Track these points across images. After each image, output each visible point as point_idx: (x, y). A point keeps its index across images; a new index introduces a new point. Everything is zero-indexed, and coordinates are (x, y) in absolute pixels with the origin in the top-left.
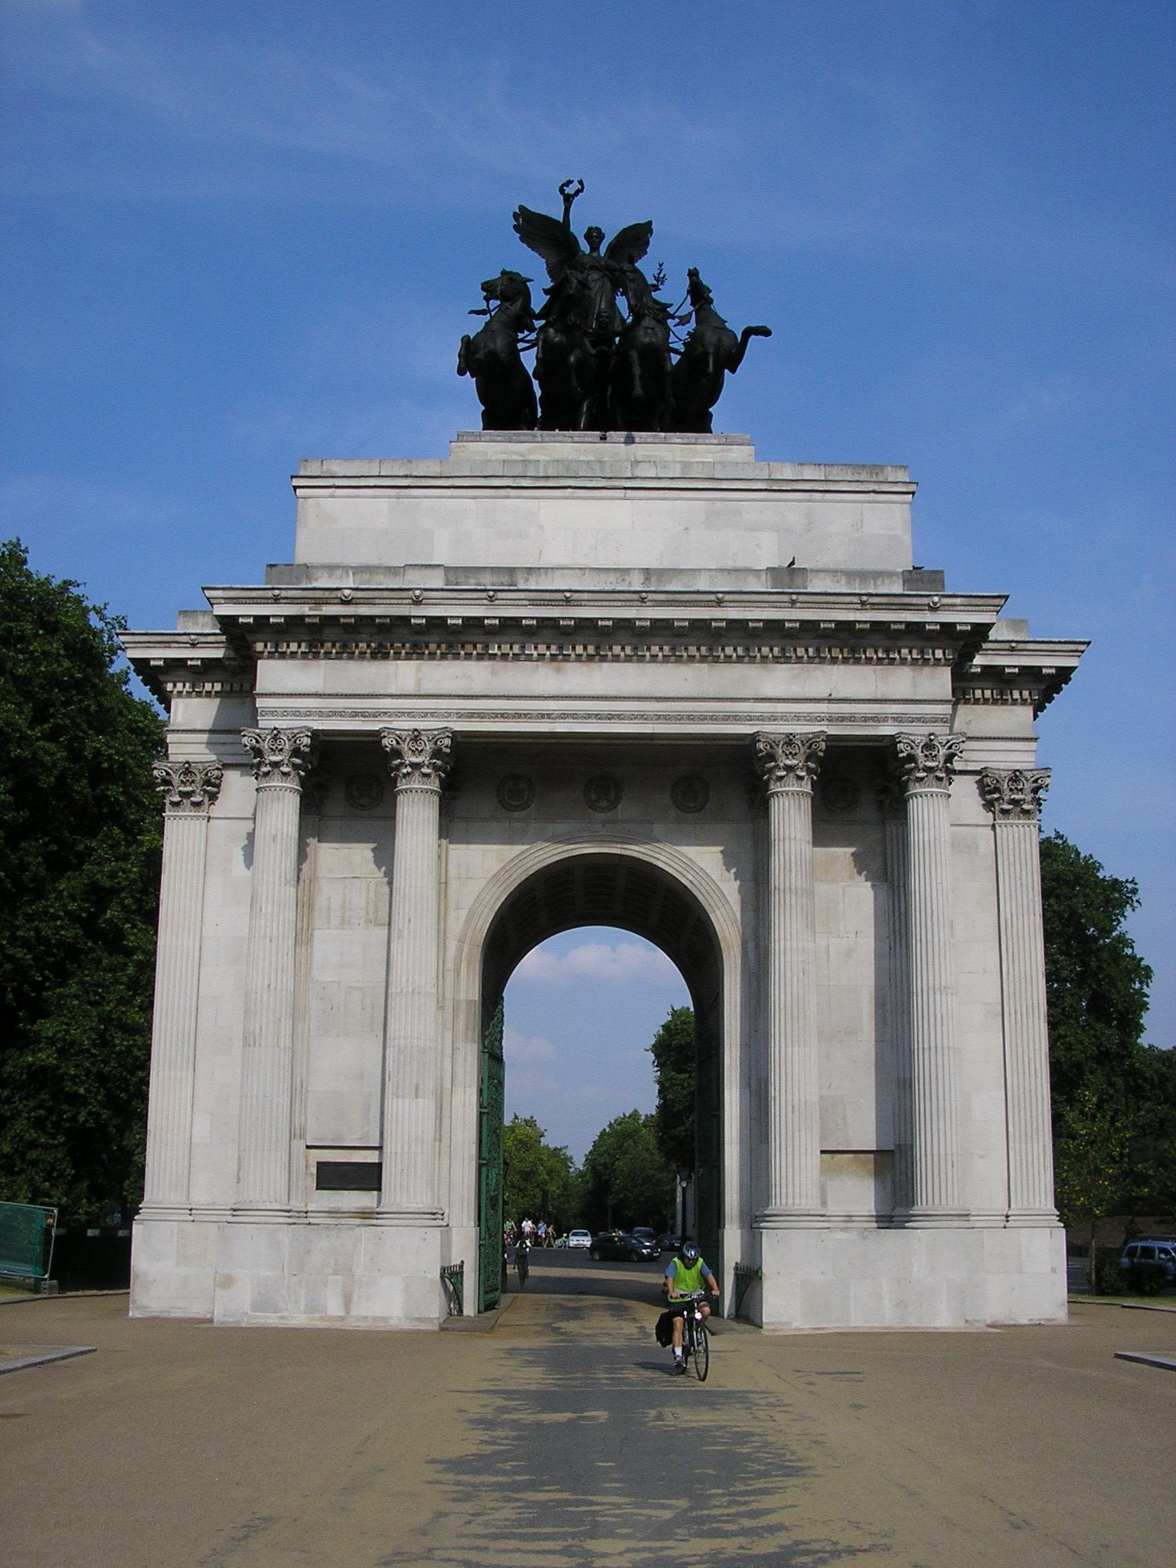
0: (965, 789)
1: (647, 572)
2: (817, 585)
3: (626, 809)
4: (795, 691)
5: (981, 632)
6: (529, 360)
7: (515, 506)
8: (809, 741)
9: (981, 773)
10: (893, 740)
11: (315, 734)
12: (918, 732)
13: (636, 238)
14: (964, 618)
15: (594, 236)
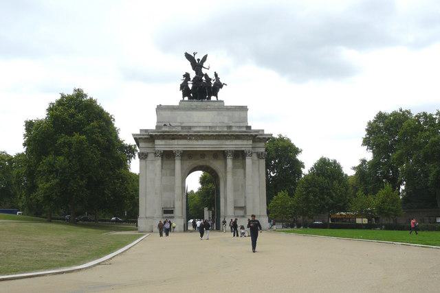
0: (255, 156)
1: (210, 127)
2: (234, 129)
3: (206, 159)
4: (231, 143)
5: (256, 135)
6: (190, 86)
7: (189, 112)
8: (232, 151)
9: (257, 153)
10: (243, 151)
11: (164, 151)
12: (247, 149)
13: (205, 58)
14: (254, 134)
15: (198, 60)
